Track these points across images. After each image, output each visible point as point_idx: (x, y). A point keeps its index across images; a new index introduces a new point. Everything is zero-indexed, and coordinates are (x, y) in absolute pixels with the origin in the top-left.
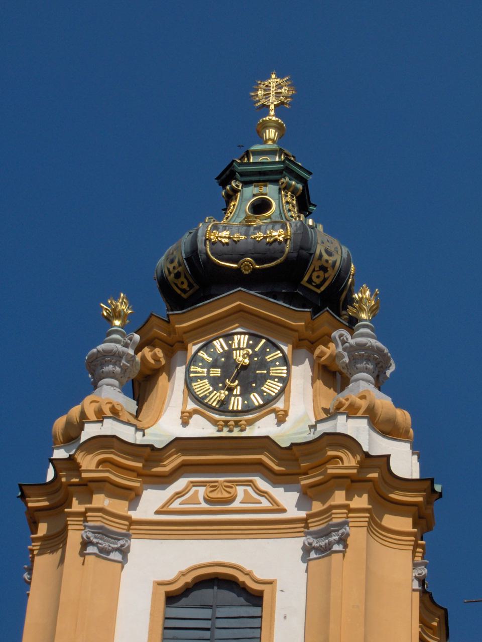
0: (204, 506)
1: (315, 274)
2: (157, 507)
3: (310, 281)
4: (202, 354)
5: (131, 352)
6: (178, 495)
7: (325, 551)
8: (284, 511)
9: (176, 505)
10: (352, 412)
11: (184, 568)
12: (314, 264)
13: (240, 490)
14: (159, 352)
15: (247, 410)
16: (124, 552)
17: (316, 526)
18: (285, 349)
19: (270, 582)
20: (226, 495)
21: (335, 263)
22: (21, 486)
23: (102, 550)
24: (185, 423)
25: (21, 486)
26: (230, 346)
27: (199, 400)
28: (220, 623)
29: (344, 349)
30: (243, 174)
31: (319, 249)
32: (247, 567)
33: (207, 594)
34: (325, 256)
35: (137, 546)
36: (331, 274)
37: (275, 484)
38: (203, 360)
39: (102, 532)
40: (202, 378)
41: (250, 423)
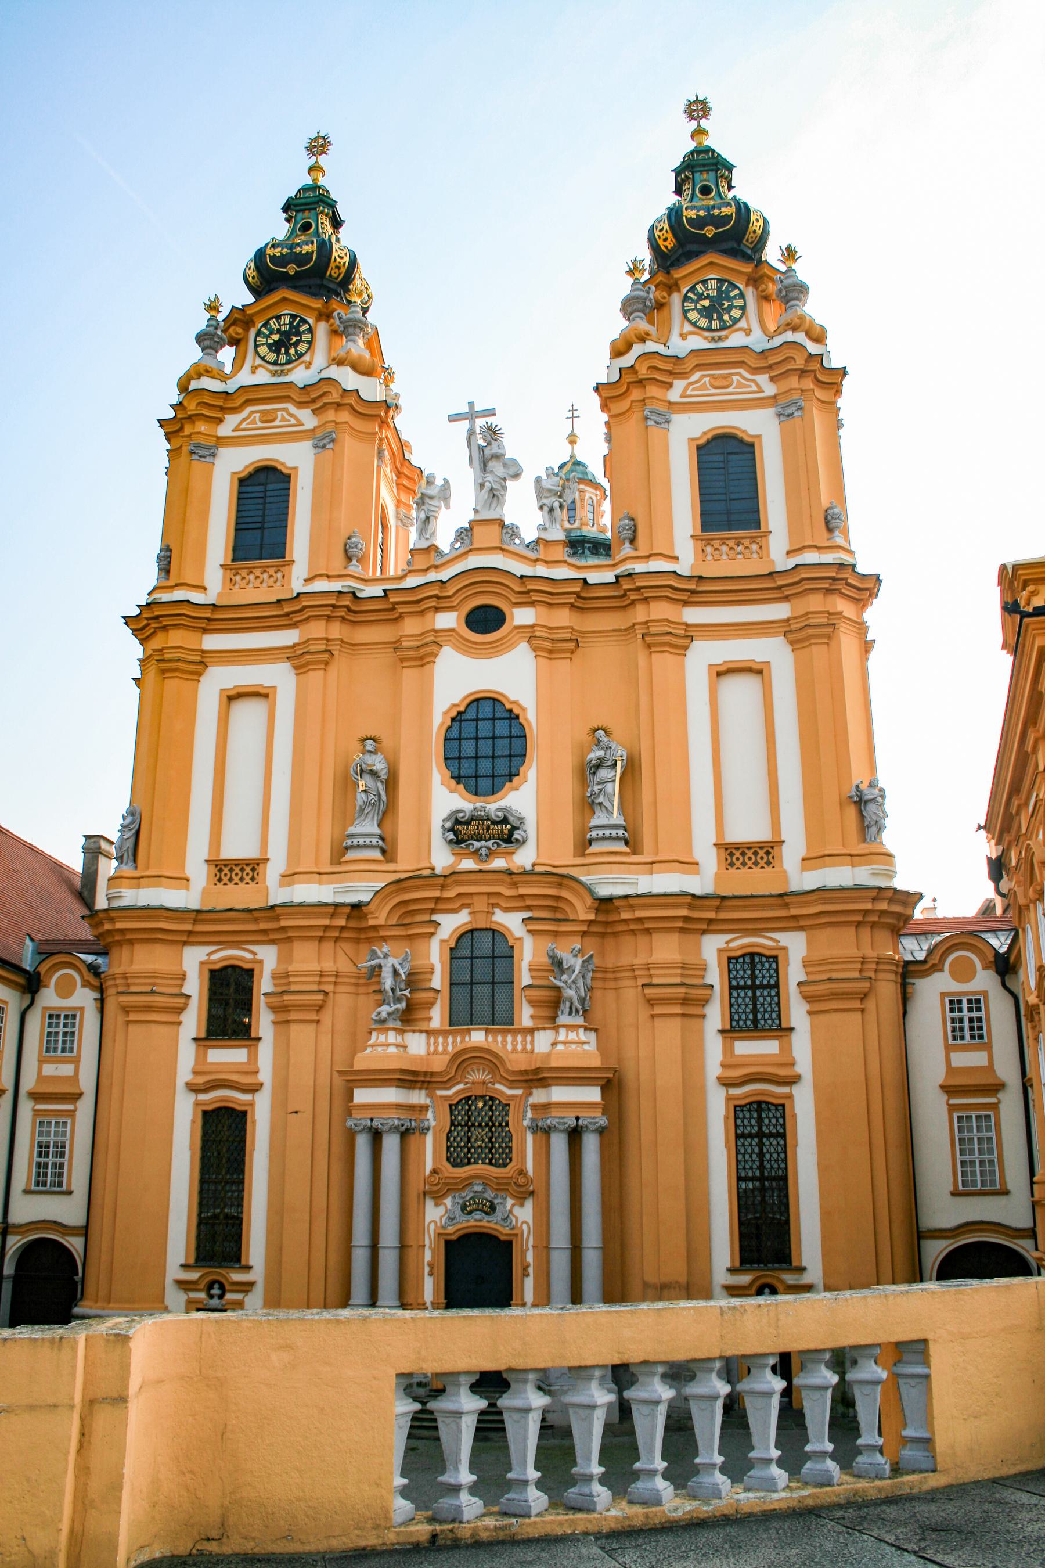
0: (260, 425)
1: (333, 272)
2: (233, 426)
3: (331, 275)
4: (263, 330)
5: (219, 332)
6: (244, 420)
7: (324, 447)
8: (303, 425)
9: (243, 426)
10: (340, 363)
11: (247, 463)
12: (332, 265)
13: (279, 414)
14: (239, 330)
15: (289, 362)
16: (214, 455)
17: (319, 434)
18: (311, 321)
19: (295, 469)
20: (270, 418)
21: (345, 263)
22: (158, 420)
23: (200, 457)
24: (254, 372)
25: (158, 420)
26: (279, 323)
27: (263, 358)
28: (268, 493)
29: (341, 323)
30: (296, 205)
31: (335, 255)
32: (282, 460)
33: (262, 477)
34: (338, 260)
35: (224, 452)
36: (343, 270)
37: (299, 408)
38: (264, 333)
39: (198, 446)
40: (263, 344)
41: (290, 370)
